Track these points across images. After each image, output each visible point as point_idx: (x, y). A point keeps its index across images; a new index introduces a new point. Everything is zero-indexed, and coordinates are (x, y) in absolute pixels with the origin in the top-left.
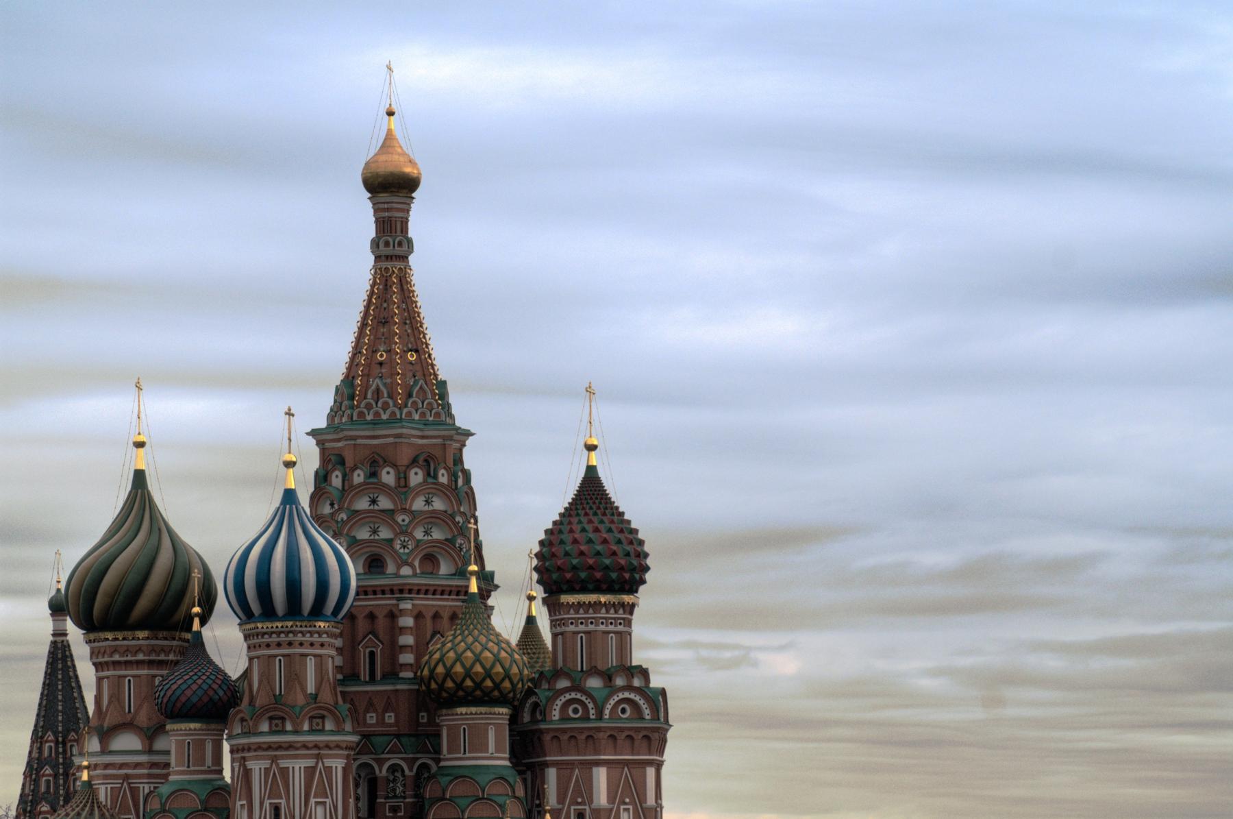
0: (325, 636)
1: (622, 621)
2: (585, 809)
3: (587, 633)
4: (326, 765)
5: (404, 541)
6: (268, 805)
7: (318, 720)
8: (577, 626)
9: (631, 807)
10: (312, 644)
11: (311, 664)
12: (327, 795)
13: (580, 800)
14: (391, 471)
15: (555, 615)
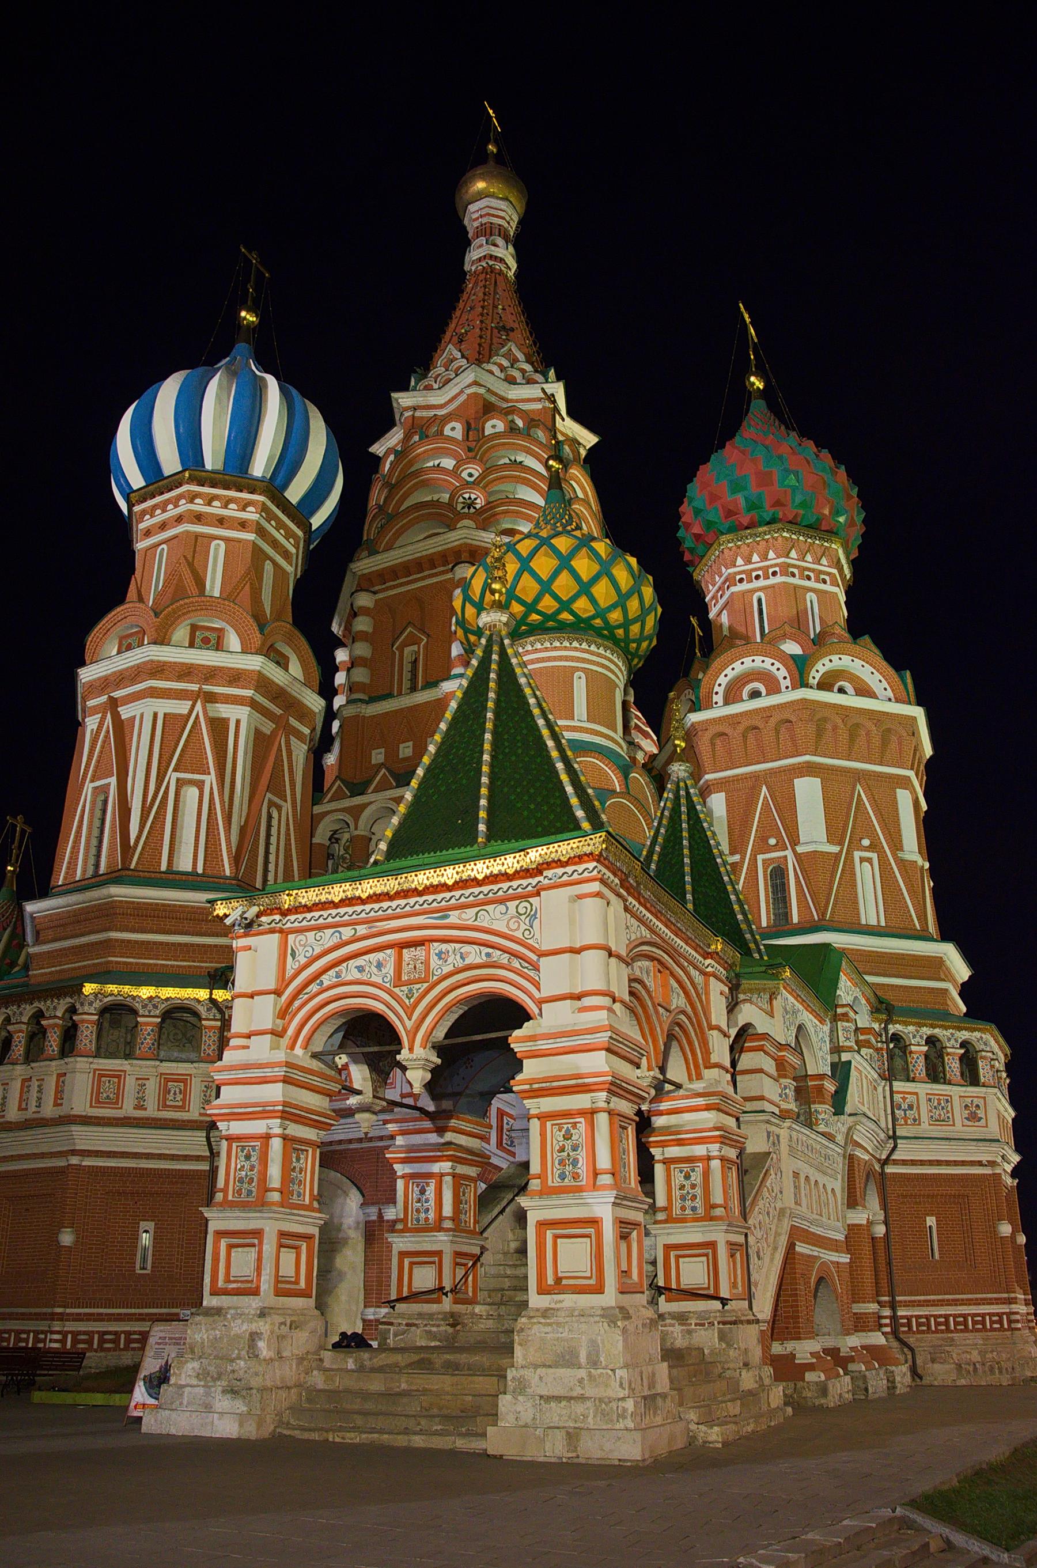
0: (251, 509)
1: (827, 578)
2: (786, 857)
3: (773, 586)
4: (211, 714)
5: (470, 498)
6: (90, 790)
7: (207, 634)
8: (750, 581)
9: (874, 856)
10: (221, 522)
11: (218, 552)
12: (208, 768)
13: (772, 841)
14: (459, 426)
15: (714, 585)
